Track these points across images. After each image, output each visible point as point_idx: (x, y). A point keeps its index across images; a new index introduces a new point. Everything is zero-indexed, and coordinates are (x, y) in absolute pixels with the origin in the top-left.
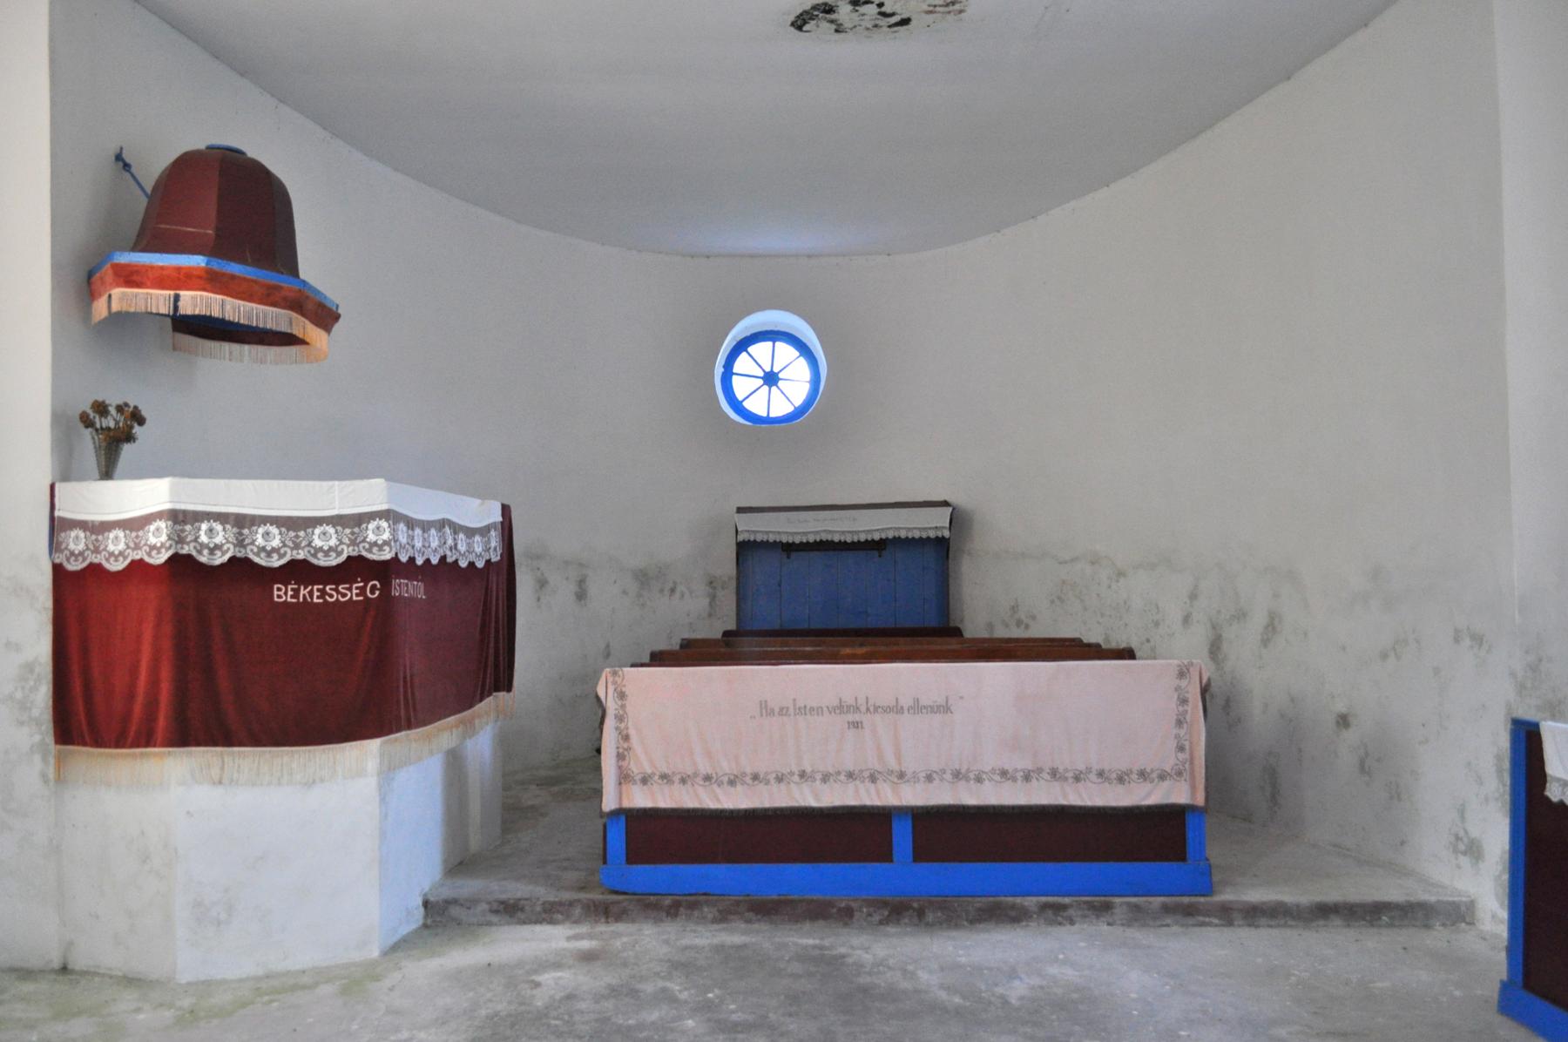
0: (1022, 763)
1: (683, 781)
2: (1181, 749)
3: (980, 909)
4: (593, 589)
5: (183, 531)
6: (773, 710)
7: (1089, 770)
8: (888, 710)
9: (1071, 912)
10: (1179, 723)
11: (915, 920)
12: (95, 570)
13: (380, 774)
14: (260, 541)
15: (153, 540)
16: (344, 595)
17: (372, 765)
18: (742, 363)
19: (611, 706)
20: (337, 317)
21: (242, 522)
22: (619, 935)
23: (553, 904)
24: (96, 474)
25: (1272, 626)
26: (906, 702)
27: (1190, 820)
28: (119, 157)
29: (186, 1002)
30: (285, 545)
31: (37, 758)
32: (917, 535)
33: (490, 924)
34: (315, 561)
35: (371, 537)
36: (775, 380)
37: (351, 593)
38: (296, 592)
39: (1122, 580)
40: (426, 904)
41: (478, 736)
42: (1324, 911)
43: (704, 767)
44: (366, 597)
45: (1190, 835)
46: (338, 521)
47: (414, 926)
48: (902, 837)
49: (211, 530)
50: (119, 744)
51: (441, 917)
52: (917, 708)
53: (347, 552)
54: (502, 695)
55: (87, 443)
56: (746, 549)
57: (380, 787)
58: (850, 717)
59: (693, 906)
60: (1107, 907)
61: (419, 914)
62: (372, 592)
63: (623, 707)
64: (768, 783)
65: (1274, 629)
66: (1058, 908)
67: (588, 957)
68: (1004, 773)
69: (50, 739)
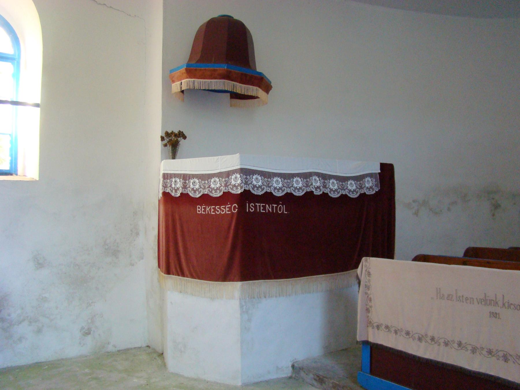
1: (396, 332)
5: (167, 182)
6: (443, 295)
14: (192, 186)
16: (223, 211)
17: (237, 294)
21: (185, 177)
30: (201, 188)
33: (313, 385)
34: (211, 195)
35: (233, 183)
37: (225, 210)
38: (205, 208)
40: (293, 366)
44: (233, 213)
46: (219, 175)
47: (284, 376)
53: (223, 189)
57: (241, 307)
58: (494, 309)
61: (288, 372)
62: (234, 210)
63: (369, 281)
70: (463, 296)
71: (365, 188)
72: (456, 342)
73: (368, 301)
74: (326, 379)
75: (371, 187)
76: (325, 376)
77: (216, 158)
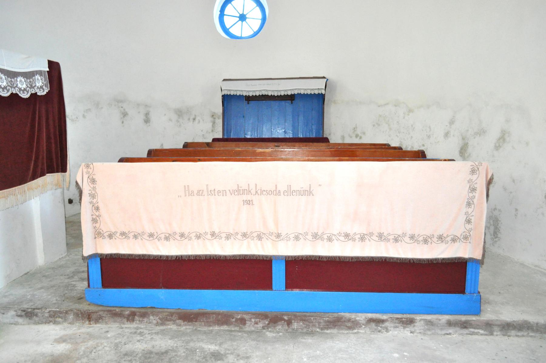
0: (357, 229)
1: (135, 237)
3: (328, 321)
4: (153, 117)
6: (193, 192)
7: (404, 235)
8: (269, 193)
9: (387, 324)
10: (469, 204)
11: (286, 327)
19: (86, 189)
22: (91, 336)
23: (55, 312)
25: (503, 138)
26: (282, 187)
27: (470, 267)
33: (16, 324)
39: (411, 114)
43: (149, 229)
45: (468, 277)
48: (279, 274)
52: (290, 192)
56: (227, 99)
58: (245, 197)
59: (144, 315)
60: (411, 322)
63: (94, 188)
64: (190, 239)
65: (504, 140)
68: (347, 235)
70: (214, 190)
71: (36, 88)
72: (209, 233)
73: (94, 211)
74: (38, 311)
75: (41, 87)
76: (33, 307)
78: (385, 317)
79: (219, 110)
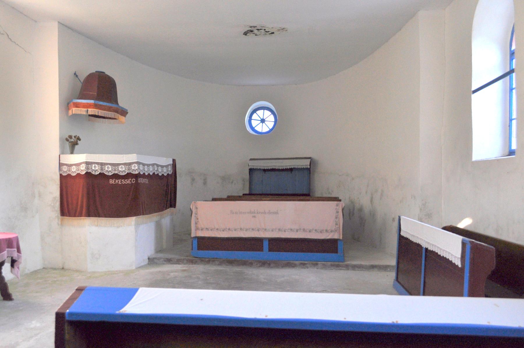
1: (211, 230)
2: (337, 224)
7: (313, 229)
9: (308, 265)
10: (336, 218)
12: (69, 175)
13: (135, 225)
14: (106, 169)
15: (82, 169)
18: (255, 116)
19: (194, 211)
20: (127, 113)
21: (102, 164)
23: (179, 259)
24: (69, 152)
27: (339, 242)
28: (75, 74)
29: (89, 275)
31: (57, 219)
32: (300, 167)
35: (133, 168)
36: (263, 121)
37: (128, 182)
38: (115, 181)
40: (149, 259)
41: (166, 218)
42: (373, 267)
43: (217, 227)
46: (125, 164)
48: (266, 244)
49: (95, 166)
50: (75, 216)
51: (152, 261)
53: (127, 172)
54: (172, 209)
55: (67, 145)
56: (251, 171)
59: (213, 261)
60: (317, 264)
66: (304, 264)
67: (184, 271)
68: (291, 230)
69: (59, 215)
77: (122, 155)
78: (306, 262)
79: (247, 177)
